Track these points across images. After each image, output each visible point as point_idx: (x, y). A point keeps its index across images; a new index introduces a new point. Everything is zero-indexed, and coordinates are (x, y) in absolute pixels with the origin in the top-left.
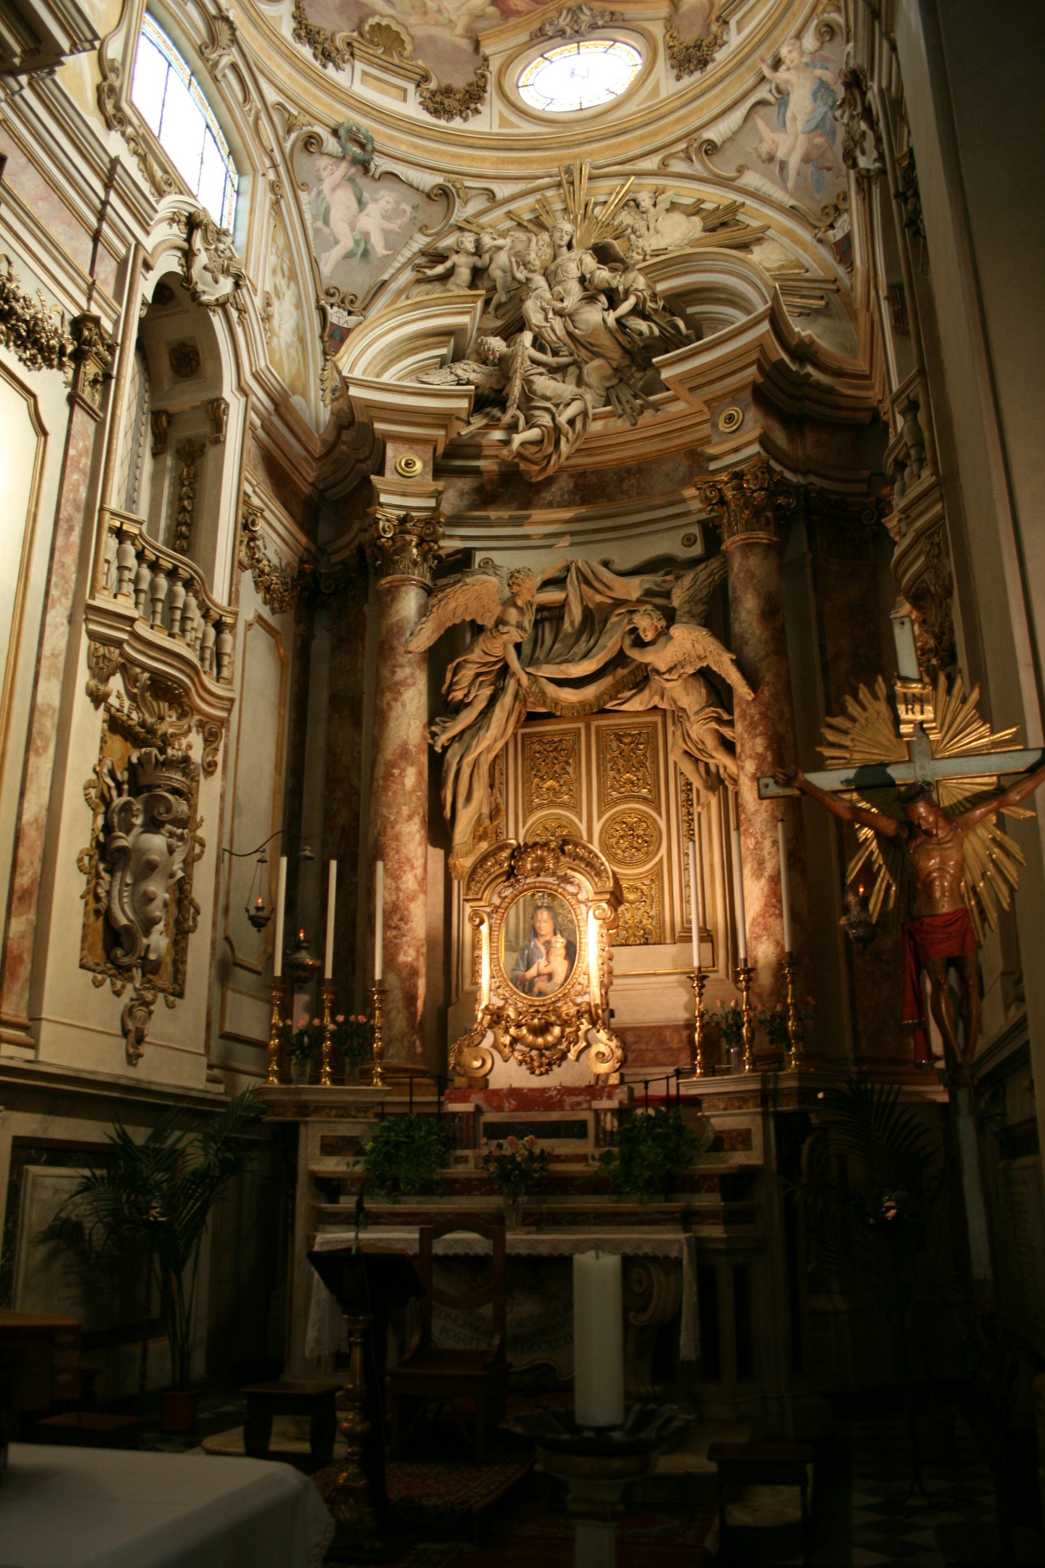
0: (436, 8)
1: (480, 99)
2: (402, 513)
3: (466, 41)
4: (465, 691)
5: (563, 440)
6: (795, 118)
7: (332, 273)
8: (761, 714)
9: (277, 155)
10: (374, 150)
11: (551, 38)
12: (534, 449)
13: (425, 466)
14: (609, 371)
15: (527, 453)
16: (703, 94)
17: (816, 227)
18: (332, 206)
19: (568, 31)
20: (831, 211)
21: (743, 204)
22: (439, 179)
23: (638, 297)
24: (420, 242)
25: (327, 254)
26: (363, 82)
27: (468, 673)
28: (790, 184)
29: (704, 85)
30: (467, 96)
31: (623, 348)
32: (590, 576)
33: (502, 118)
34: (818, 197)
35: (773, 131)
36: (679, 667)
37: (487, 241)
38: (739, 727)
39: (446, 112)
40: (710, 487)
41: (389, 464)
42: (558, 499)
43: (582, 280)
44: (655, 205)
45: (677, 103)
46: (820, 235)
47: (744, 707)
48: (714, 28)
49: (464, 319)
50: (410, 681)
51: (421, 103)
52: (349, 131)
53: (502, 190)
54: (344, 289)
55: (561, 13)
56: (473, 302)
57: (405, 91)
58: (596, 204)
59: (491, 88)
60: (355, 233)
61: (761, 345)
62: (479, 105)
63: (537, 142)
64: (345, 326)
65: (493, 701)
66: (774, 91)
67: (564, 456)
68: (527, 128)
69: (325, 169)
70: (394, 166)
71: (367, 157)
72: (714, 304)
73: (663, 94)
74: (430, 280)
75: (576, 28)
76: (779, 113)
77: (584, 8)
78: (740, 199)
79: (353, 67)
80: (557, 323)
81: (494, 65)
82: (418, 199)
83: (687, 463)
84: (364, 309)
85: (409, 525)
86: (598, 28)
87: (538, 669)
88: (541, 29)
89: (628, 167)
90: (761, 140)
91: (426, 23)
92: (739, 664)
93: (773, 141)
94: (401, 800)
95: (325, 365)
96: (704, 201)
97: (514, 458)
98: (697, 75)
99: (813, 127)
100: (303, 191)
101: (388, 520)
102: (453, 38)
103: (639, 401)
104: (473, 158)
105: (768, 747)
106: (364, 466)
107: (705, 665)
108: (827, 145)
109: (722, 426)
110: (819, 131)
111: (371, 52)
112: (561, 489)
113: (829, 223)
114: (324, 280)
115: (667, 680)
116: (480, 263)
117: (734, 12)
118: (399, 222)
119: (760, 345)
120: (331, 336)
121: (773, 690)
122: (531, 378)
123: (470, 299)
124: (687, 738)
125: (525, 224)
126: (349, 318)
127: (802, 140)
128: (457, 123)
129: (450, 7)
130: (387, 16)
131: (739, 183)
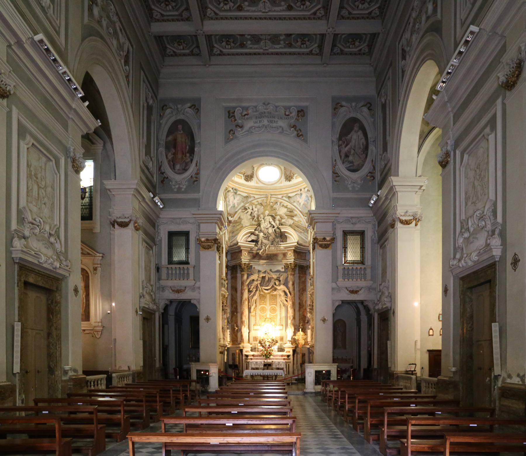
24: (242, 204)
27: (252, 287)
37: (254, 208)
43: (270, 222)
48: (292, 174)
53: (256, 197)
65: (256, 291)
68: (260, 185)
80: (266, 230)
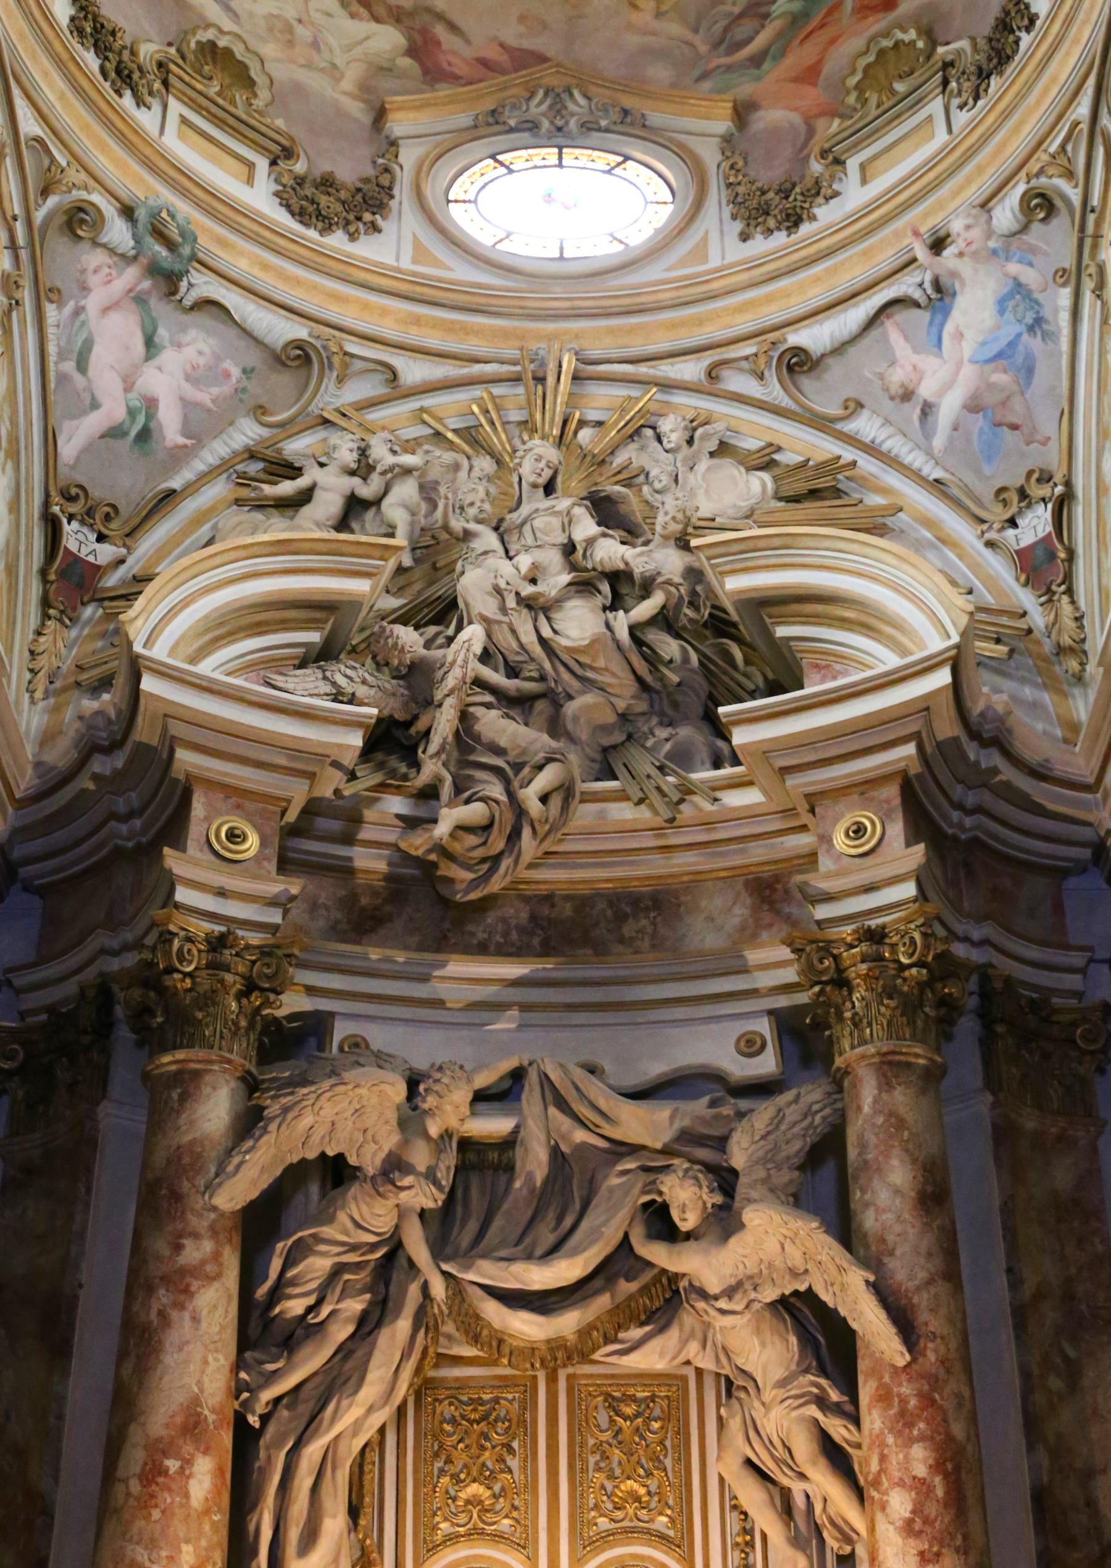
0: (310, 40)
1: (380, 207)
2: (219, 929)
3: (361, 105)
4: (311, 1300)
5: (526, 833)
6: (960, 335)
7: (78, 459)
8: (920, 1395)
9: (19, 228)
10: (194, 258)
11: (511, 130)
12: (472, 840)
13: (263, 843)
14: (612, 718)
15: (457, 848)
16: (791, 271)
17: (983, 521)
18: (97, 339)
19: (546, 124)
20: (1015, 498)
21: (854, 463)
22: (300, 331)
23: (668, 594)
25: (74, 423)
26: (181, 136)
27: (318, 1265)
28: (938, 442)
29: (795, 257)
30: (359, 197)
31: (639, 679)
32: (570, 1096)
33: (418, 247)
34: (988, 470)
35: (916, 351)
36: (748, 1286)
37: (380, 452)
38: (874, 1420)
39: (319, 215)
40: (820, 949)
41: (195, 831)
42: (499, 938)
43: (569, 549)
44: (690, 442)
45: (744, 277)
46: (992, 535)
47: (887, 1379)
48: (816, 167)
49: (360, 586)
50: (209, 1268)
51: (277, 194)
52: (155, 215)
54: (95, 493)
55: (533, 94)
56: (381, 559)
57: (251, 166)
58: (582, 423)
59: (403, 192)
60: (132, 395)
61: (927, 709)
62: (378, 217)
63: (483, 300)
64: (91, 559)
66: (927, 285)
67: (526, 858)
68: (463, 272)
69: (95, 271)
70: (223, 291)
71: (177, 267)
72: (830, 626)
73: (714, 261)
74: (260, 506)
75: (559, 122)
76: (931, 323)
77: (576, 93)
78: (848, 454)
79: (165, 107)
81: (409, 156)
82: (253, 358)
83: (748, 901)
84: (127, 535)
85: (227, 954)
86: (599, 130)
87: (467, 1268)
88: (493, 112)
89: (643, 369)
90: (893, 363)
91: (292, 61)
92: (883, 1292)
93: (915, 367)
94: (179, 1528)
95: (43, 625)
96: (779, 449)
97: (429, 851)
98: (780, 238)
99: (990, 354)
100: (52, 302)
101: (189, 940)
102: (336, 96)
103: (670, 779)
104: (366, 306)
105: (937, 1467)
106: (124, 828)
107: (802, 1288)
108: (1015, 388)
109: (840, 841)
110: (1002, 362)
111: (199, 86)
112: (504, 920)
113: (1007, 516)
114: (62, 470)
115: (723, 1312)
116: (366, 491)
117: (856, 147)
118: (215, 391)
119: (924, 707)
120: (62, 574)
121: (942, 1350)
122: (472, 709)
123: (378, 553)
124: (752, 1433)
125: (450, 435)
126: (97, 546)
127: (968, 372)
128: (337, 240)
129: (333, 41)
130: (229, 33)
131: (849, 427)
